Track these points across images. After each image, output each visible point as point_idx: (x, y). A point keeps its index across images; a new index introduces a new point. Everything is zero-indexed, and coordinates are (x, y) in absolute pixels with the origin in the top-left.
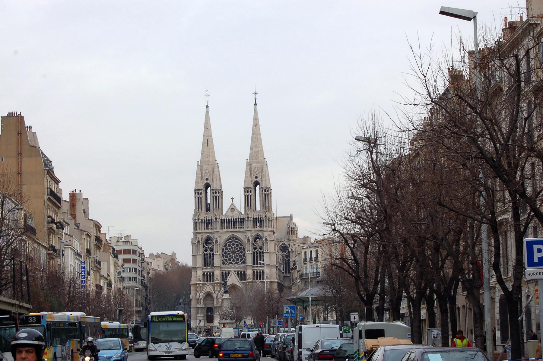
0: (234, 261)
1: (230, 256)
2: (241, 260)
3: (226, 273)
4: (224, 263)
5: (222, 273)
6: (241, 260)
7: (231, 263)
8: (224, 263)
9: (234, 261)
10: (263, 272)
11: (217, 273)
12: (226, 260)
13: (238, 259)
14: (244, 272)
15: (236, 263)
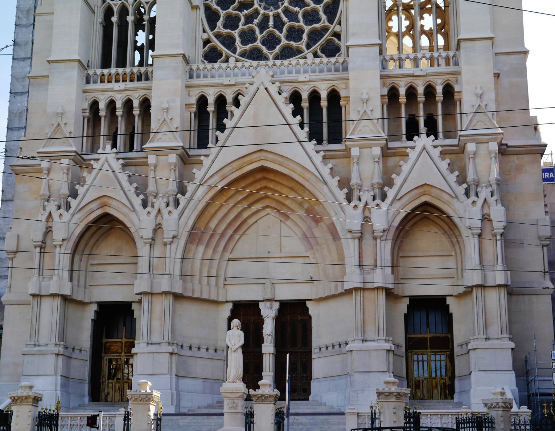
0: (271, 41)
1: (249, 19)
2: (314, 36)
3: (221, 100)
4: (212, 56)
5: (202, 101)
6: (314, 36)
7: (255, 55)
8: (212, 56)
9: (271, 41)
10: (448, 90)
11: (169, 96)
12: (229, 42)
13: (295, 34)
14: (334, 96)
15: (288, 53)
